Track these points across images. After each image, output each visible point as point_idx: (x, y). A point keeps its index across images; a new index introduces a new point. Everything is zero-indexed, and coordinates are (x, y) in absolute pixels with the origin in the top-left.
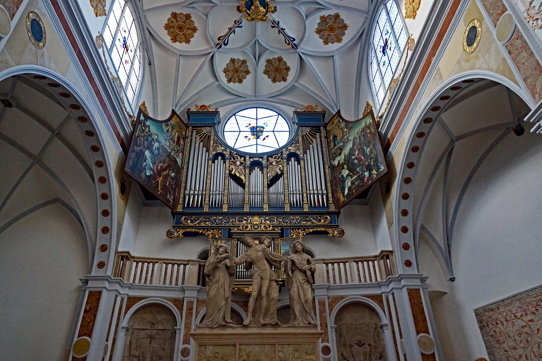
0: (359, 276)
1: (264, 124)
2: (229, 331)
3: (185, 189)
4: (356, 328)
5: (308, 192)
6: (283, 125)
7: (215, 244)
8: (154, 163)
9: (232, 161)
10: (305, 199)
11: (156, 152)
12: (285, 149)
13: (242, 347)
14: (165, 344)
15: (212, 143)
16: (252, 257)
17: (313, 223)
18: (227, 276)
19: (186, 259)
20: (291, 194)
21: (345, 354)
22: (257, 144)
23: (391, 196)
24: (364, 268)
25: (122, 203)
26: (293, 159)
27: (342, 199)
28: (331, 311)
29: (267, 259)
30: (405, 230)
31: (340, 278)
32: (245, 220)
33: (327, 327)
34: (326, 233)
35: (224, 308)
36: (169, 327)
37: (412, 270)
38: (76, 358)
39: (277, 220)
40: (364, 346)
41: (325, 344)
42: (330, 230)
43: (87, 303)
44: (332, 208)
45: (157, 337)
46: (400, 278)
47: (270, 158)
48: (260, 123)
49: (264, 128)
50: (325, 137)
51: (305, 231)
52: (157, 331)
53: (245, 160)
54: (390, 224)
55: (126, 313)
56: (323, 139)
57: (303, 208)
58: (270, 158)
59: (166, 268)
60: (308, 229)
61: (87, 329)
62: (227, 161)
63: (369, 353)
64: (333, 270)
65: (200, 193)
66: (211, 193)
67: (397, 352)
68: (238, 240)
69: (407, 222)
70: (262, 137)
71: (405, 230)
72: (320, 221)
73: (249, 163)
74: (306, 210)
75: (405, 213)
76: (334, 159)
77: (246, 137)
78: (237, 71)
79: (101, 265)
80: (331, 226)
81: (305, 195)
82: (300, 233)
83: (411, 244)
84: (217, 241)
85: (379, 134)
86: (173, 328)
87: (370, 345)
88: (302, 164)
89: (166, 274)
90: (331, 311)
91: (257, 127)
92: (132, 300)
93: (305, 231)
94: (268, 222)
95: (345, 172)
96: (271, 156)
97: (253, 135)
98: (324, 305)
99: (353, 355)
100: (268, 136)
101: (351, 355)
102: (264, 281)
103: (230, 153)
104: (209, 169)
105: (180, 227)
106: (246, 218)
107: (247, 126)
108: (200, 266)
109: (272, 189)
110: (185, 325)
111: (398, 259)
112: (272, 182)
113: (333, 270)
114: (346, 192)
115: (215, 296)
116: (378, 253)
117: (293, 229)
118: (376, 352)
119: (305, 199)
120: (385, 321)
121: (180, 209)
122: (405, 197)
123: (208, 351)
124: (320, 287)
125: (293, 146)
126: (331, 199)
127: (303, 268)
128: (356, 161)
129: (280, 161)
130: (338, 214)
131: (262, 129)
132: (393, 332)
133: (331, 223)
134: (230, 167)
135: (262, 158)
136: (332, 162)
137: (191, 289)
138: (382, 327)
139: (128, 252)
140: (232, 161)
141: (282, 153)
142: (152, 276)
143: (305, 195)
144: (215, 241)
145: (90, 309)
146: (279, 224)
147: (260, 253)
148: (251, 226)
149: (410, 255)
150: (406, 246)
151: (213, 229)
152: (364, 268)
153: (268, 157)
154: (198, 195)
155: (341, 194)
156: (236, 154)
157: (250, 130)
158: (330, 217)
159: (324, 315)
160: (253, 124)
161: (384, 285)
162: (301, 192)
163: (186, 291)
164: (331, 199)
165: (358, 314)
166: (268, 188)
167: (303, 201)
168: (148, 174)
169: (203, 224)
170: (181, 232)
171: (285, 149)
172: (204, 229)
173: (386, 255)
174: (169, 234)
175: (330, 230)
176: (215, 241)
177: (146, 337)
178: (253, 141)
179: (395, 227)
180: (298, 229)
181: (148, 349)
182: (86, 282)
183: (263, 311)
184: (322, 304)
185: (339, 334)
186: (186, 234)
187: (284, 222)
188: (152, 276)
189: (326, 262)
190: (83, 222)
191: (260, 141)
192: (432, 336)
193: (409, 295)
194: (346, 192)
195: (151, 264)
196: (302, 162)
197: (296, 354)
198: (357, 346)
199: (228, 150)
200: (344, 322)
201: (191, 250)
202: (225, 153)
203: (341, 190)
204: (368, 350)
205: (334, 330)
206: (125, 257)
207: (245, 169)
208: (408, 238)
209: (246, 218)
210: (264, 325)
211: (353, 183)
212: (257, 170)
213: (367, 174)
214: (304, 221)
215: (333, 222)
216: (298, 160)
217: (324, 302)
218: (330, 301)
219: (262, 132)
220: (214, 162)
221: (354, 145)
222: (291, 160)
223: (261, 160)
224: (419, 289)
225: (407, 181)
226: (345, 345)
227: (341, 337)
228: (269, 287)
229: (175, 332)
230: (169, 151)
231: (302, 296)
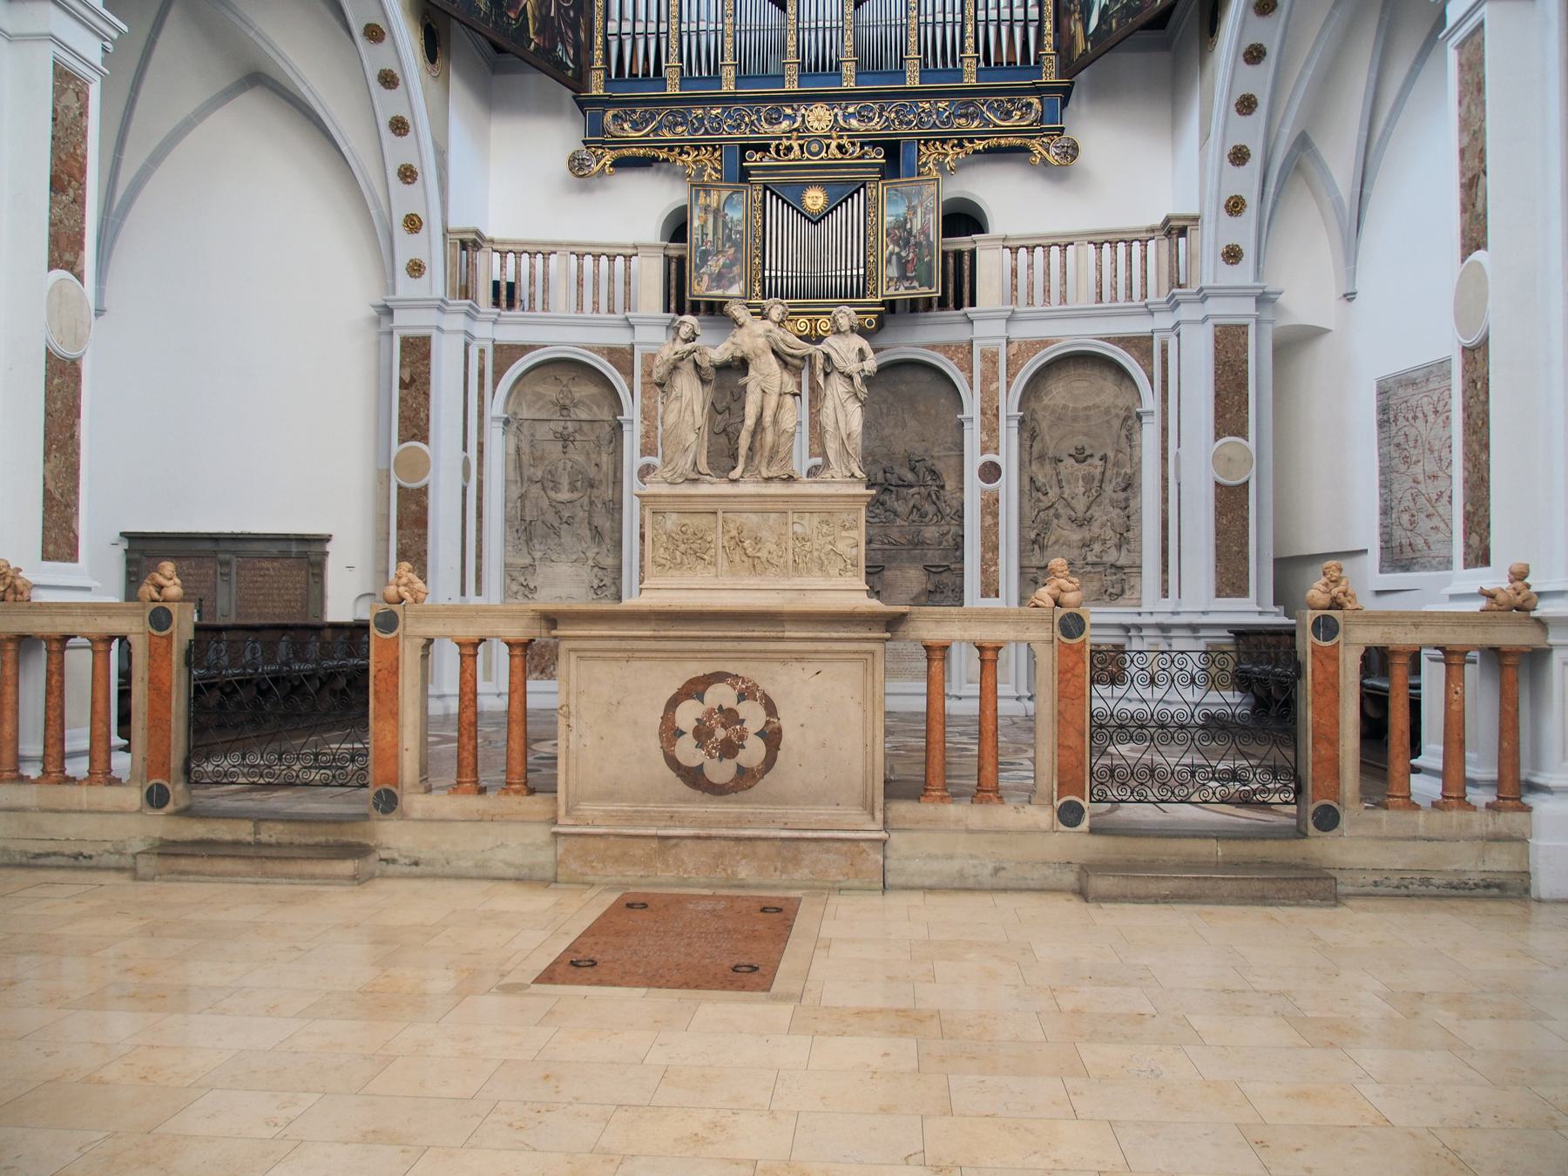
0: (1100, 285)
2: (704, 489)
3: (607, 18)
4: (1075, 419)
5: (981, 15)
7: (702, 201)
10: (970, 42)
13: (729, 515)
14: (599, 453)
16: (745, 349)
17: (988, 122)
18: (697, 383)
19: (630, 240)
20: (926, 24)
21: (1041, 479)
23: (1217, 50)
24: (1115, 261)
25: (435, 88)
27: (1080, 45)
28: (1011, 375)
29: (774, 352)
30: (1239, 156)
31: (1047, 291)
32: (787, 117)
33: (997, 416)
34: (1024, 150)
35: (694, 447)
36: (606, 415)
37: (1242, 275)
38: (406, 489)
39: (880, 116)
40: (1089, 461)
42: (1035, 145)
43: (402, 366)
44: (1049, 76)
45: (578, 437)
46: (1203, 296)
51: (962, 147)
52: (577, 425)
54: (1205, 136)
55: (495, 384)
57: (958, 74)
59: (580, 267)
60: (971, 141)
61: (415, 425)
63: (1098, 477)
64: (1030, 266)
65: (652, 28)
66: (684, 27)
67: (1165, 479)
68: (766, 188)
69: (1250, 131)
72: (1008, 115)
74: (970, 80)
75: (1246, 105)
79: (416, 269)
80: (1041, 130)
81: (970, 29)
82: (946, 155)
83: (1252, 200)
84: (708, 193)
86: (615, 416)
87: (1104, 458)
89: (580, 283)
90: (1011, 375)
92: (506, 354)
93: (962, 147)
94: (854, 123)
98: (995, 363)
99: (1060, 481)
101: (1054, 482)
102: (767, 398)
105: (604, 142)
106: (788, 111)
108: (668, 259)
110: (643, 411)
111: (1207, 241)
113: (1030, 266)
115: (676, 425)
116: (1158, 221)
117: (927, 141)
118: (1118, 474)
119: (970, 42)
120: (1150, 402)
121: (597, 89)
123: (669, 523)
126: (1049, 39)
127: (847, 370)
130: (1066, 93)
133: (1041, 121)
137: (649, 323)
138: (1139, 417)
139: (477, 233)
142: (545, 290)
143: (970, 29)
144: (702, 194)
145: (413, 380)
146: (888, 127)
147: (761, 342)
148: (801, 146)
149: (1242, 231)
150: (1235, 205)
151: (698, 148)
152: (1115, 261)
154: (646, 35)
158: (1041, 100)
159: (993, 387)
161: (1160, 311)
162: (958, 18)
164: (1049, 39)
165: (1085, 384)
167: (962, 51)
170: (608, 158)
172: (671, 149)
173: (1175, 229)
174: (577, 165)
175: (1035, 145)
176: (702, 194)
177: (551, 437)
179: (1217, 151)
180: (943, 142)
181: (561, 465)
182: (387, 311)
183: (766, 454)
184: (990, 359)
185: (1028, 428)
186: (621, 164)
187: (901, 123)
188: (545, 290)
189: (1010, 244)
190: (344, 149)
192: (1251, 444)
193: (1216, 341)
195: (539, 256)
197: (825, 529)
198: (1072, 461)
200: (1046, 401)
201: (637, 208)
203: (1081, 12)
204: (1099, 470)
205: (1015, 423)
206: (471, 244)
208: (1245, 181)
209: (788, 111)
210: (768, 479)
214: (961, 116)
215: (1047, 116)
217: (997, 354)
218: (1014, 349)
224: (1246, 326)
226: (1042, 457)
227: (1033, 437)
228: (779, 406)
229: (621, 426)
231: (842, 425)
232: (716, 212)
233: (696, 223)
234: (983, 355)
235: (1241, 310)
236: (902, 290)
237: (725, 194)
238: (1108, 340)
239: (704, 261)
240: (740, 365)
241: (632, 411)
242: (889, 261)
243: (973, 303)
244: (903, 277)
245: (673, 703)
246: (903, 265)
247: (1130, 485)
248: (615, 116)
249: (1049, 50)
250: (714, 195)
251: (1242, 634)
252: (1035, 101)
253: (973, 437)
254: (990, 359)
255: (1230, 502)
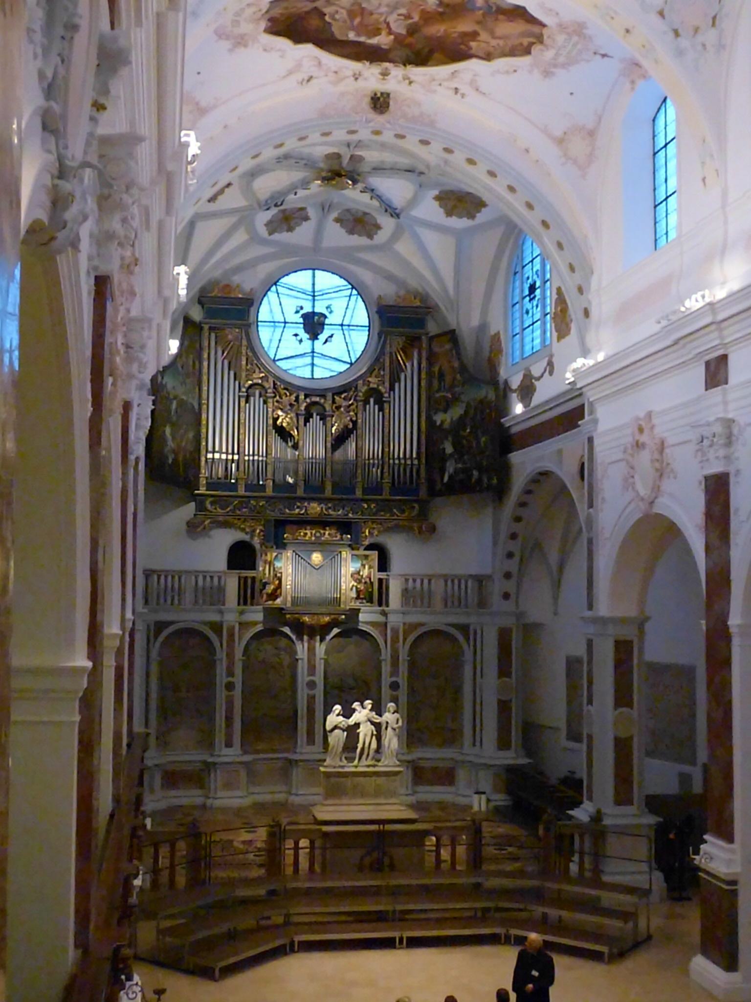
1: (327, 308)
6: (360, 315)
8: (174, 438)
9: (277, 401)
10: (386, 475)
11: (174, 419)
12: (361, 382)
15: (244, 363)
17: (393, 514)
22: (313, 352)
26: (372, 400)
27: (438, 486)
30: (510, 555)
32: (298, 507)
41: (394, 679)
44: (423, 493)
47: (337, 398)
48: (320, 308)
49: (325, 317)
50: (427, 359)
53: (297, 398)
56: (424, 364)
58: (337, 398)
62: (270, 400)
70: (322, 337)
71: (510, 555)
72: (403, 512)
73: (305, 404)
74: (386, 495)
76: (435, 413)
77: (296, 335)
78: (288, 219)
81: (386, 470)
84: (266, 555)
85: (502, 425)
88: (387, 411)
91: (314, 313)
92: (160, 626)
94: (331, 512)
95: (449, 449)
96: (339, 394)
97: (306, 331)
100: (331, 336)
103: (275, 384)
104: (242, 414)
106: (299, 504)
107: (297, 312)
109: (338, 454)
111: (497, 588)
112: (340, 440)
114: (446, 479)
122: (518, 519)
124: (395, 612)
125: (374, 375)
128: (465, 442)
129: (352, 404)
131: (322, 319)
132: (475, 668)
134: (273, 411)
135: (323, 396)
136: (432, 413)
140: (277, 401)
141: (356, 388)
149: (510, 586)
153: (333, 395)
155: (438, 479)
156: (285, 389)
157: (301, 320)
160: (308, 309)
163: (225, 614)
166: (332, 453)
168: (170, 461)
169: (238, 512)
171: (361, 382)
173: (480, 580)
178: (307, 345)
180: (373, 523)
184: (395, 631)
191: (318, 344)
194: (446, 479)
196: (386, 406)
199: (271, 380)
202: (266, 385)
207: (297, 415)
208: (513, 566)
209: (299, 504)
210: (368, 766)
211: (456, 471)
212: (316, 418)
213: (475, 473)
216: (380, 402)
219: (322, 325)
220: (247, 401)
221: (466, 412)
222: (369, 403)
223: (322, 401)
225: (523, 505)
230: (184, 398)
232: (270, 563)
233: (261, 569)
234: (392, 629)
235: (508, 622)
236: (358, 604)
237: (275, 554)
238: (449, 625)
239: (264, 588)
240: (357, 725)
241: (221, 655)
242: (352, 589)
243: (387, 606)
244: (358, 598)
245: (362, 858)
246: (358, 592)
247: (458, 690)
248: (212, 503)
249: (423, 481)
250: (269, 555)
251: (511, 770)
252: (416, 506)
253: (386, 668)
254: (395, 631)
255: (504, 707)
